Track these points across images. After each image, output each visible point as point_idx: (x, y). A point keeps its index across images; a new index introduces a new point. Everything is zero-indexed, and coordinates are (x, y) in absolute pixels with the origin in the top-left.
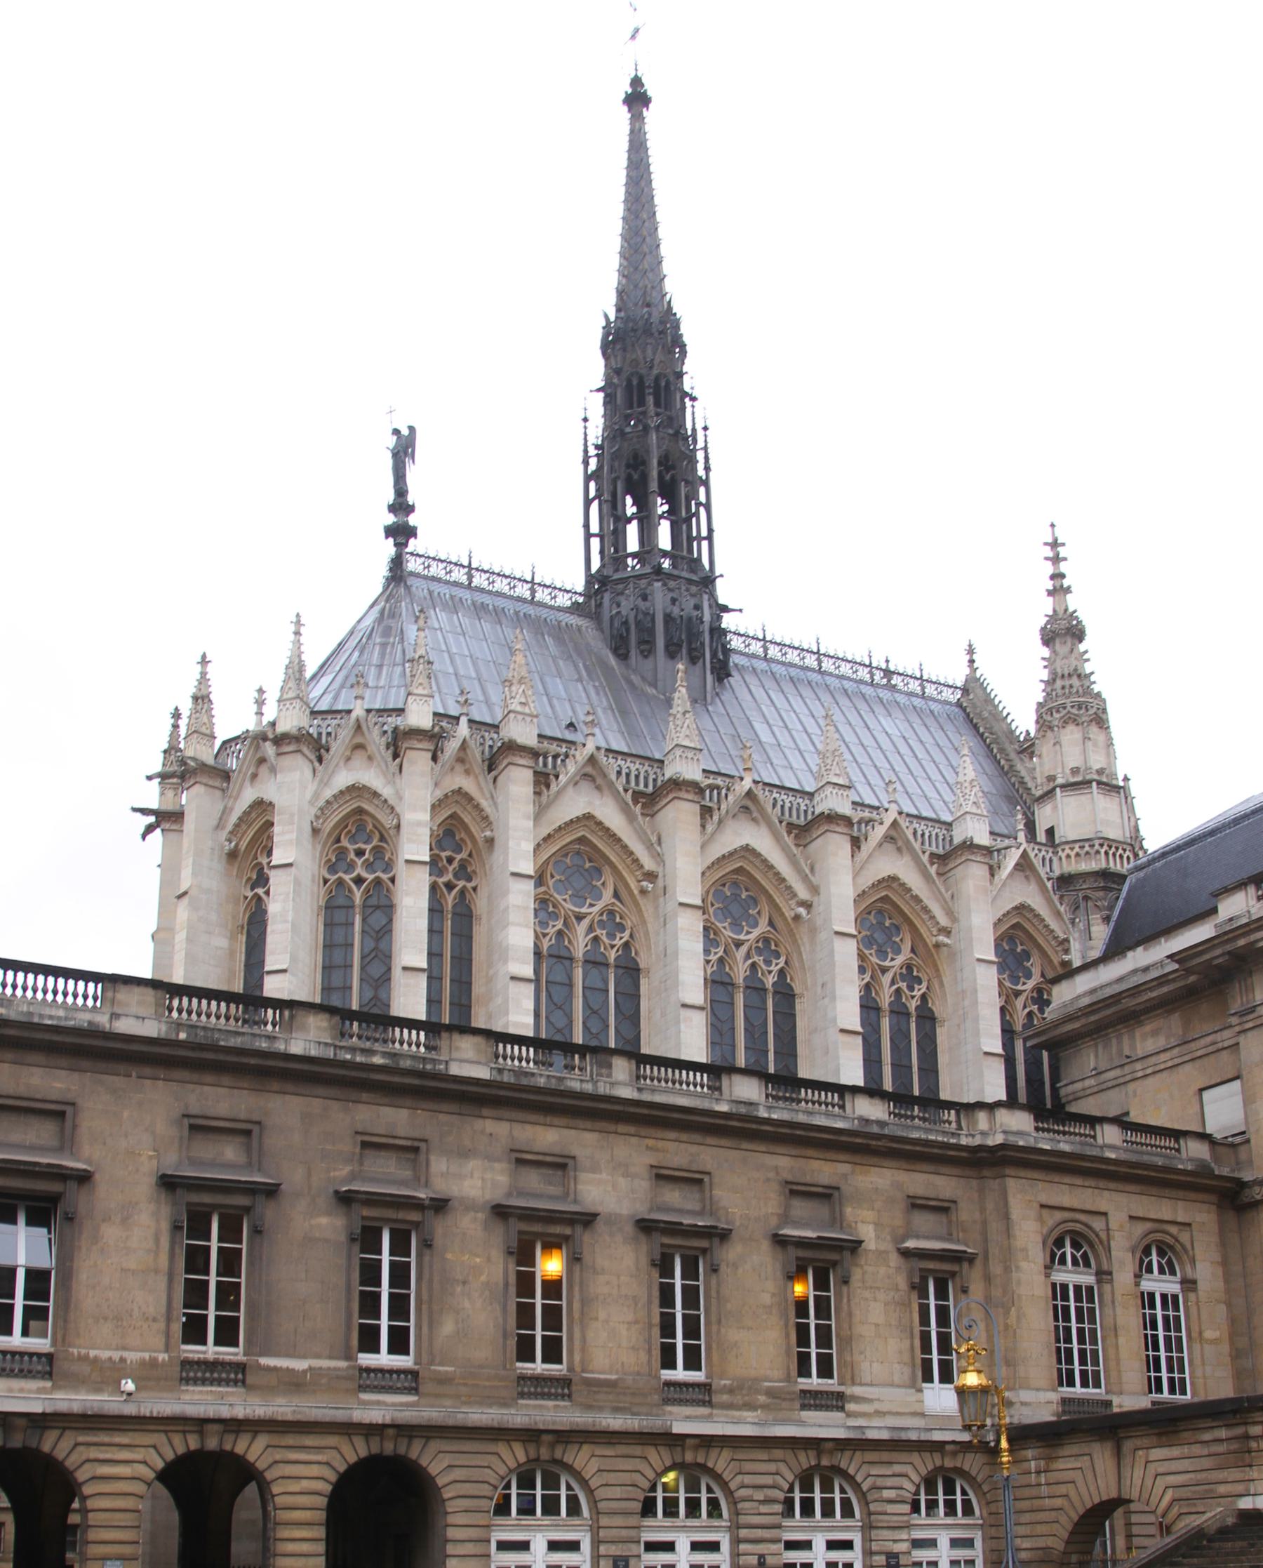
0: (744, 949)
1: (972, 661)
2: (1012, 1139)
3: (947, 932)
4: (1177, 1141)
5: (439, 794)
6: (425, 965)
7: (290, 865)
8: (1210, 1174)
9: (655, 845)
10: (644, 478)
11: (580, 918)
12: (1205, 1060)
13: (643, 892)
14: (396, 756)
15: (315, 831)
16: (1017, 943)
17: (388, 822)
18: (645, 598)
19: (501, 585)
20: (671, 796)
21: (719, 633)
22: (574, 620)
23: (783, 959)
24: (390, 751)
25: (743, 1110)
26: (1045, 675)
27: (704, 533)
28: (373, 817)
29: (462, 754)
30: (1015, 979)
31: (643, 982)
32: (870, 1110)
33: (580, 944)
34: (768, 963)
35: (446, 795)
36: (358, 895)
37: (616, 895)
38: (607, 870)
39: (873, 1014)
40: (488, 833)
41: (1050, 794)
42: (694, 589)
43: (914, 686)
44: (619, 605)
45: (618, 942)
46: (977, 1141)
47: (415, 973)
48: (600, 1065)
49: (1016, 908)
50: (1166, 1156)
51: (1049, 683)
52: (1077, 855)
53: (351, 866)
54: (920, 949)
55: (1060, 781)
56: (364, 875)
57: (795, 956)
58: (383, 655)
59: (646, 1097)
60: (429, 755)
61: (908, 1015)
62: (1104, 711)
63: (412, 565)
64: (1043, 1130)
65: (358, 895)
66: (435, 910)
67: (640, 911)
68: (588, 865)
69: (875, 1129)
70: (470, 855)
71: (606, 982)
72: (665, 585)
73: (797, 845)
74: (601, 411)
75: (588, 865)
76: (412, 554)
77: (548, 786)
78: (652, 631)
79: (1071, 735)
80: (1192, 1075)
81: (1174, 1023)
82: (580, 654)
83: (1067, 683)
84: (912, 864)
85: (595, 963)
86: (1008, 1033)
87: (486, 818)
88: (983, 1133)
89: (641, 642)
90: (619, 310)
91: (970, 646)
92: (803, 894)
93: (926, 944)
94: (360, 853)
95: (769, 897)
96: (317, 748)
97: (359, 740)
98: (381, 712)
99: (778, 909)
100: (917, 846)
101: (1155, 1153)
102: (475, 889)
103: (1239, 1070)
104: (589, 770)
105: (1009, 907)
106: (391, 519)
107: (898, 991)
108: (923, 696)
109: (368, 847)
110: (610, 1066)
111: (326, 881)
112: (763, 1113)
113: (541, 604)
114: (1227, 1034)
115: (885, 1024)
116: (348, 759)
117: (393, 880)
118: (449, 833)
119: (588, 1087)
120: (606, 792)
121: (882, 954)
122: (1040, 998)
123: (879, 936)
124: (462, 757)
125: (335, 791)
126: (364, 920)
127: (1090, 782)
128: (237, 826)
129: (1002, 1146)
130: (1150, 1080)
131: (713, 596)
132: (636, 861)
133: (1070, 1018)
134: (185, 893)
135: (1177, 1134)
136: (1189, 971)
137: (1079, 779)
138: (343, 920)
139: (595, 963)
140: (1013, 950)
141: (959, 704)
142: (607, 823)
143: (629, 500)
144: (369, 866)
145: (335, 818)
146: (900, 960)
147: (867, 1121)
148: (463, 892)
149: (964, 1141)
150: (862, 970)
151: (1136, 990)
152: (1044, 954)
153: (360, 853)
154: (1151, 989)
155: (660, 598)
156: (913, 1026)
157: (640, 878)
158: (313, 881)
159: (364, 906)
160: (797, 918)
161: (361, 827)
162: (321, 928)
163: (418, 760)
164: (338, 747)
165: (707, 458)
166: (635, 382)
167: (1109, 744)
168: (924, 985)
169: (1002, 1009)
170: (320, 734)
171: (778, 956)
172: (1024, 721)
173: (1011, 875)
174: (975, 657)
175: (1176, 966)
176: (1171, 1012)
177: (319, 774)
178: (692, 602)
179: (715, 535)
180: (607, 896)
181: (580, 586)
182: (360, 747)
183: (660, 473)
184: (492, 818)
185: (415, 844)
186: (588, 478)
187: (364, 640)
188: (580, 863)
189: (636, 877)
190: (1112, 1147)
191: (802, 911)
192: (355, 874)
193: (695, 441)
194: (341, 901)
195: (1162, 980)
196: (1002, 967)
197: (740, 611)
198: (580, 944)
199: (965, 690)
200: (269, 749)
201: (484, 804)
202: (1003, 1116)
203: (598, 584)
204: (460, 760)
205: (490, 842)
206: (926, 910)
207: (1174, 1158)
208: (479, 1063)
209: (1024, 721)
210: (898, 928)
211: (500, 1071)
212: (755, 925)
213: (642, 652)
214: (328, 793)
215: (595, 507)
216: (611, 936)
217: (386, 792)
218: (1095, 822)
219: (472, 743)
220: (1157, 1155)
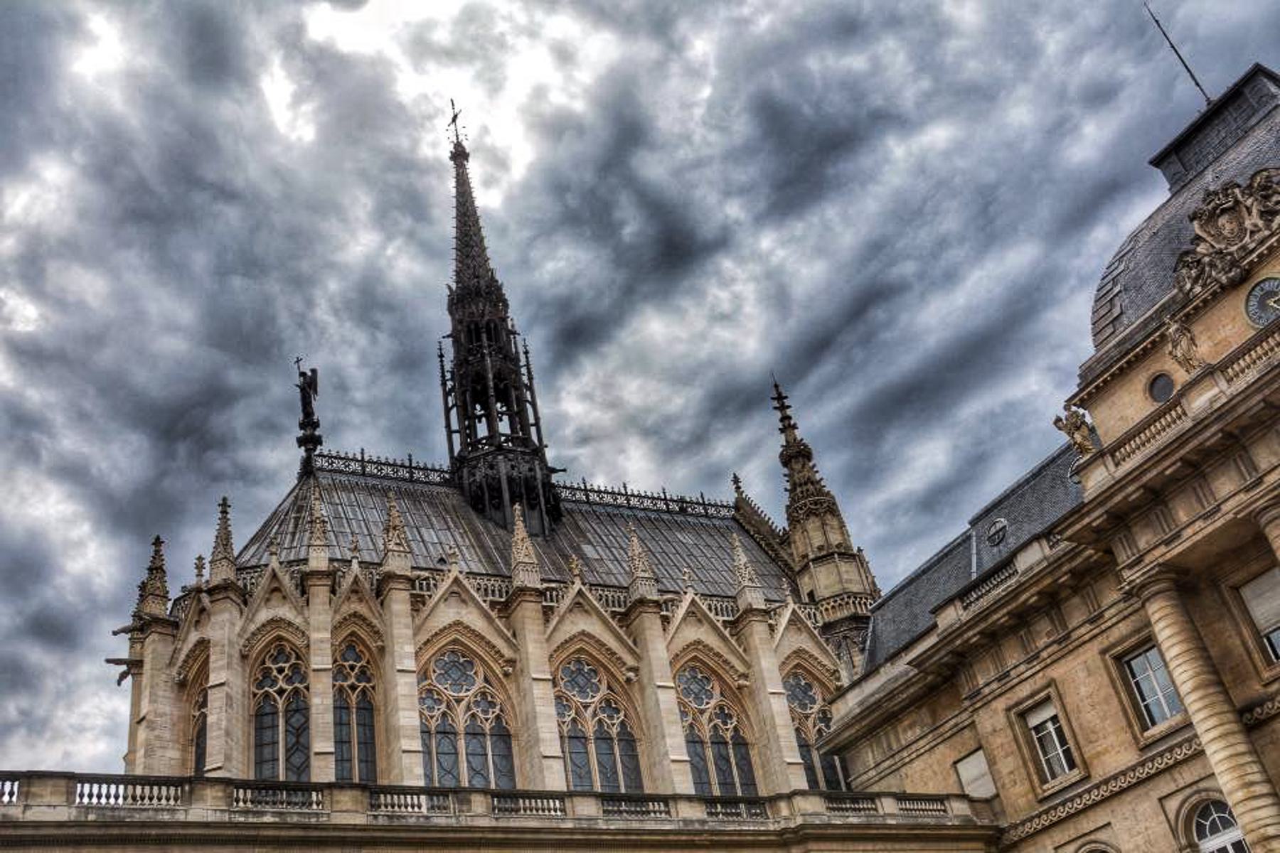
0: (590, 710)
1: (738, 488)
2: (810, 820)
3: (745, 676)
4: (942, 803)
5: (338, 618)
6: (332, 750)
7: (222, 684)
8: (976, 827)
9: (514, 639)
10: (486, 387)
11: (459, 701)
12: (954, 738)
13: (506, 675)
14: (303, 593)
15: (244, 657)
16: (800, 680)
17: (299, 642)
18: (492, 467)
19: (387, 470)
21: (549, 486)
23: (622, 714)
25: (585, 825)
26: (788, 486)
27: (532, 420)
29: (355, 587)
30: (804, 706)
31: (514, 744)
32: (692, 812)
33: (461, 720)
34: (611, 717)
35: (345, 619)
36: (281, 703)
37: (486, 680)
39: (698, 746)
40: (380, 643)
41: (806, 567)
42: (527, 458)
43: (701, 510)
46: (783, 825)
48: (461, 802)
49: (795, 652)
50: (937, 817)
51: (792, 491)
52: (833, 607)
53: (275, 682)
54: (728, 693)
55: (811, 556)
56: (285, 686)
57: (632, 711)
58: (296, 526)
59: (502, 824)
60: (327, 588)
61: (726, 743)
62: (834, 504)
63: (319, 463)
64: (834, 809)
65: (281, 703)
66: (341, 707)
68: (462, 660)
69: (697, 826)
70: (368, 662)
71: (484, 748)
73: (621, 627)
74: (452, 350)
75: (462, 660)
77: (424, 604)
78: (499, 490)
79: (812, 524)
80: (945, 753)
81: (925, 714)
82: (447, 512)
83: (805, 488)
84: (710, 630)
85: (475, 734)
86: (804, 747)
87: (377, 632)
88: (786, 819)
89: (492, 498)
90: (457, 283)
93: (731, 688)
94: (281, 671)
95: (606, 668)
96: (245, 597)
98: (290, 563)
99: (614, 676)
100: (712, 615)
101: (927, 816)
102: (373, 688)
103: (979, 741)
104: (455, 589)
105: (788, 652)
106: (301, 433)
107: (715, 726)
108: (706, 516)
109: (287, 665)
110: (469, 802)
111: (255, 695)
112: (602, 825)
113: (418, 481)
114: (965, 716)
115: (709, 753)
116: (268, 600)
117: (307, 688)
118: (351, 647)
119: (453, 822)
121: (698, 698)
122: (825, 718)
123: (695, 687)
124: (355, 590)
127: (833, 554)
128: (185, 661)
129: (802, 827)
130: (916, 763)
131: (543, 460)
132: (498, 652)
133: (847, 726)
134: (143, 718)
135: (940, 799)
136: (928, 674)
137: (824, 553)
138: (270, 724)
139: (475, 734)
140: (798, 684)
141: (734, 518)
143: (478, 407)
144: (289, 680)
145: (259, 647)
146: (713, 702)
147: (692, 822)
148: (364, 691)
149: (771, 828)
150: (684, 714)
151: (891, 695)
152: (822, 684)
153: (281, 671)
154: (902, 692)
155: (503, 468)
156: (731, 751)
158: (244, 696)
159: (286, 711)
160: (629, 680)
161: (281, 651)
162: (253, 732)
163: (320, 593)
164: (259, 592)
165: (529, 372)
166: (473, 327)
167: (842, 525)
168: (735, 719)
169: (797, 730)
170: (245, 586)
171: (618, 711)
172: (779, 521)
173: (786, 628)
175: (916, 671)
176: (919, 708)
177: (245, 615)
178: (527, 466)
179: (542, 422)
180: (479, 682)
181: (445, 463)
182: (276, 590)
183: (495, 384)
185: (321, 659)
186: (446, 394)
190: (892, 815)
191: (631, 674)
193: (519, 360)
194: (268, 709)
195: (908, 684)
196: (792, 698)
197: (564, 470)
198: (461, 720)
199: (737, 507)
200: (206, 599)
201: (375, 622)
202: (800, 802)
203: (458, 462)
204: (355, 592)
205: (382, 650)
206: (726, 662)
207: (942, 817)
208: (357, 812)
209: (779, 521)
210: (708, 679)
211: (375, 817)
212: (598, 690)
214: (252, 628)
215: (454, 412)
217: (298, 621)
218: (841, 581)
219: (361, 577)
220: (928, 817)
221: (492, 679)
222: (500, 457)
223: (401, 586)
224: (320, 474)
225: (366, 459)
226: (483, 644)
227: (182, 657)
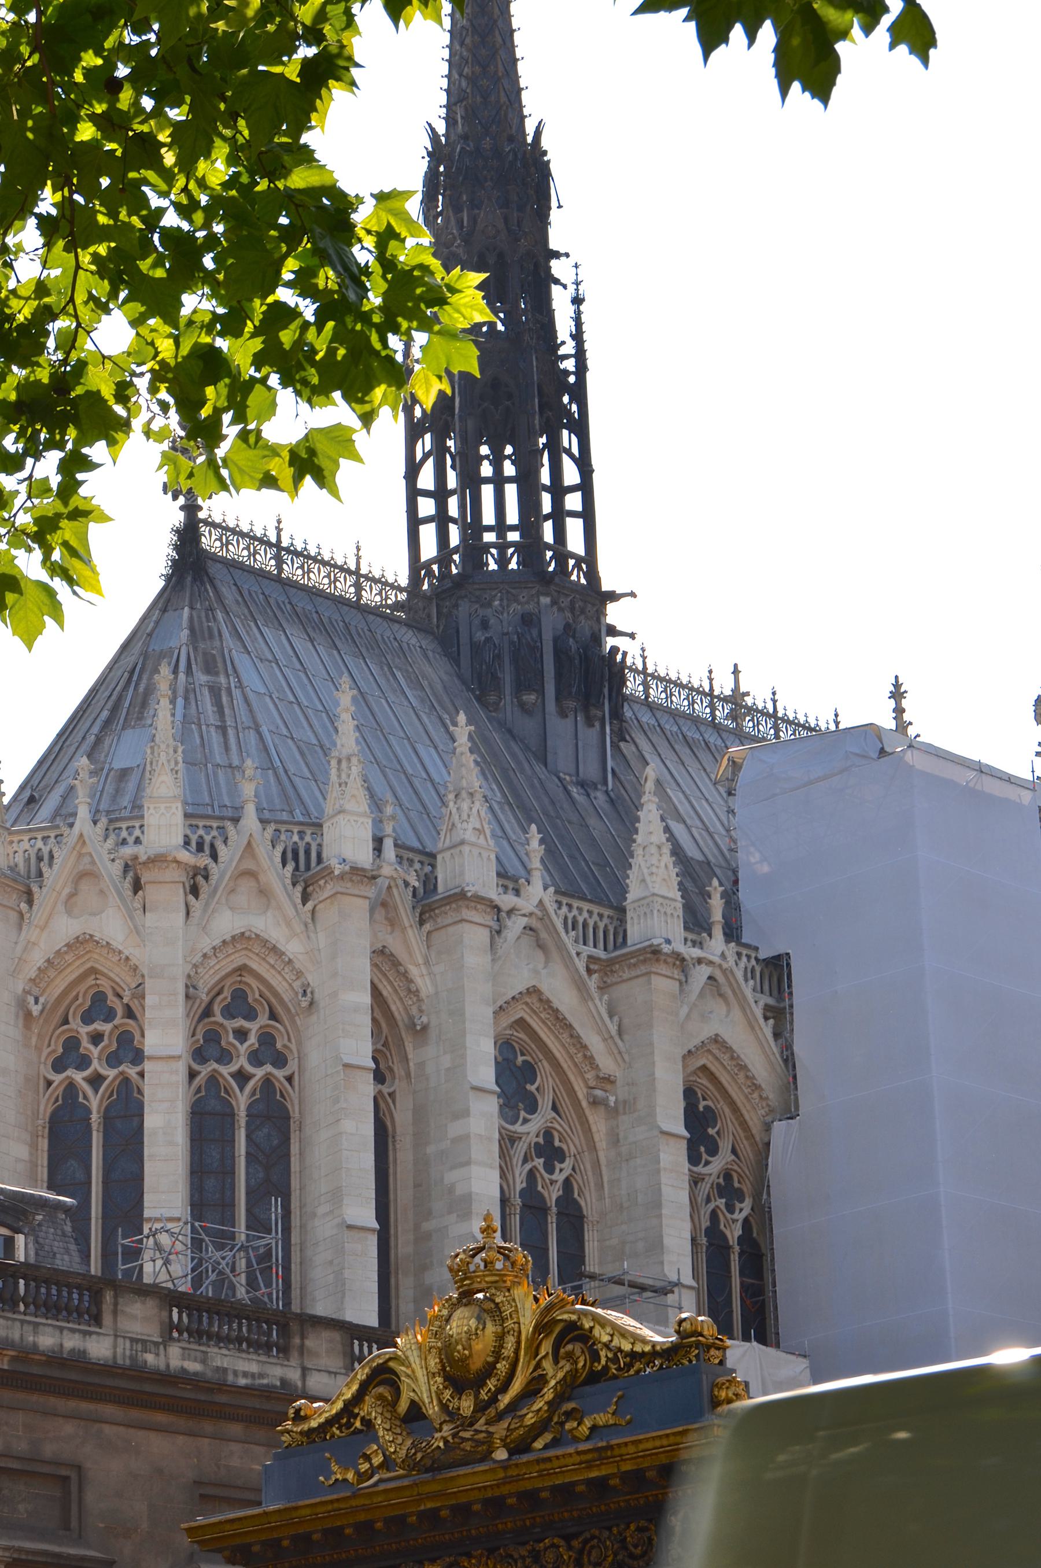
1: (899, 711)
14: (305, 898)
19: (318, 578)
20: (643, 969)
22: (410, 637)
24: (299, 888)
36: (241, 1101)
38: (544, 1067)
44: (485, 625)
45: (559, 1177)
47: (362, 1234)
56: (250, 1069)
63: (210, 541)
65: (241, 1101)
67: (588, 1131)
68: (520, 1059)
72: (554, 603)
76: (206, 522)
91: (897, 685)
97: (249, 865)
117: (289, 1079)
120: (555, 955)
125: (217, 942)
126: (247, 1136)
132: (590, 1059)
142: (556, 1004)
144: (256, 1059)
153: (242, 1035)
157: (592, 1083)
161: (240, 995)
174: (905, 703)
177: (196, 914)
184: (423, 994)
187: (182, 676)
188: (511, 1057)
189: (585, 1081)
192: (234, 1068)
201: (414, 971)
213: (522, 705)
214: (206, 944)
216: (550, 1169)
217: (293, 948)
221: (565, 1104)
222: (545, 600)
223: (477, 918)
224: (214, 569)
225: (284, 544)
226: (565, 1037)
227: (37, 958)
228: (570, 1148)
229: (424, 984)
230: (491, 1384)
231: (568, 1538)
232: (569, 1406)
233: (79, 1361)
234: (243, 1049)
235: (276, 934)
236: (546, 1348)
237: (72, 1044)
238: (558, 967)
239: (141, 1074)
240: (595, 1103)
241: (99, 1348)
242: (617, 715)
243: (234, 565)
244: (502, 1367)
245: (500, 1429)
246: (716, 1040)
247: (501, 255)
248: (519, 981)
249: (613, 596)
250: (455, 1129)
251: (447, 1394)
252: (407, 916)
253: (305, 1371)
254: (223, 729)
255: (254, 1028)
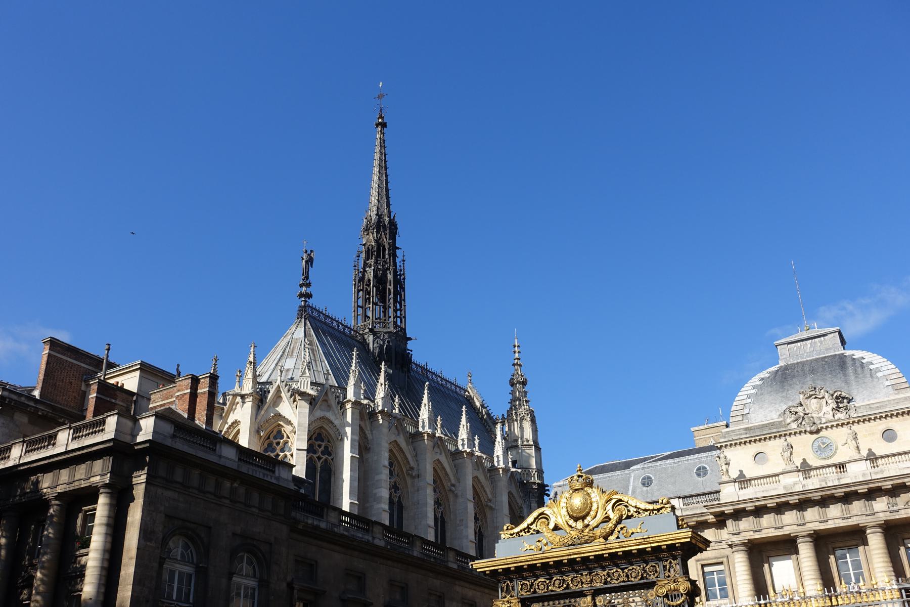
14: (341, 408)
28: (326, 431)
36: (319, 465)
63: (309, 310)
65: (319, 465)
92: (453, 482)
95: (441, 480)
132: (408, 462)
161: (319, 434)
191: (453, 488)
206: (485, 491)
214: (313, 419)
217: (336, 422)
228: (400, 487)
229: (369, 436)
230: (589, 518)
231: (623, 569)
232: (621, 526)
233: (317, 528)
234: (320, 450)
235: (332, 418)
236: (610, 506)
237: (270, 445)
238: (401, 435)
239: (292, 456)
240: (408, 474)
241: (323, 525)
242: (409, 371)
243: (314, 318)
244: (592, 513)
245: (598, 532)
246: (438, 460)
247: (384, 247)
248: (393, 438)
249: (410, 339)
250: (377, 477)
251: (571, 522)
252: (366, 417)
253: (374, 538)
254: (315, 361)
255: (323, 444)
